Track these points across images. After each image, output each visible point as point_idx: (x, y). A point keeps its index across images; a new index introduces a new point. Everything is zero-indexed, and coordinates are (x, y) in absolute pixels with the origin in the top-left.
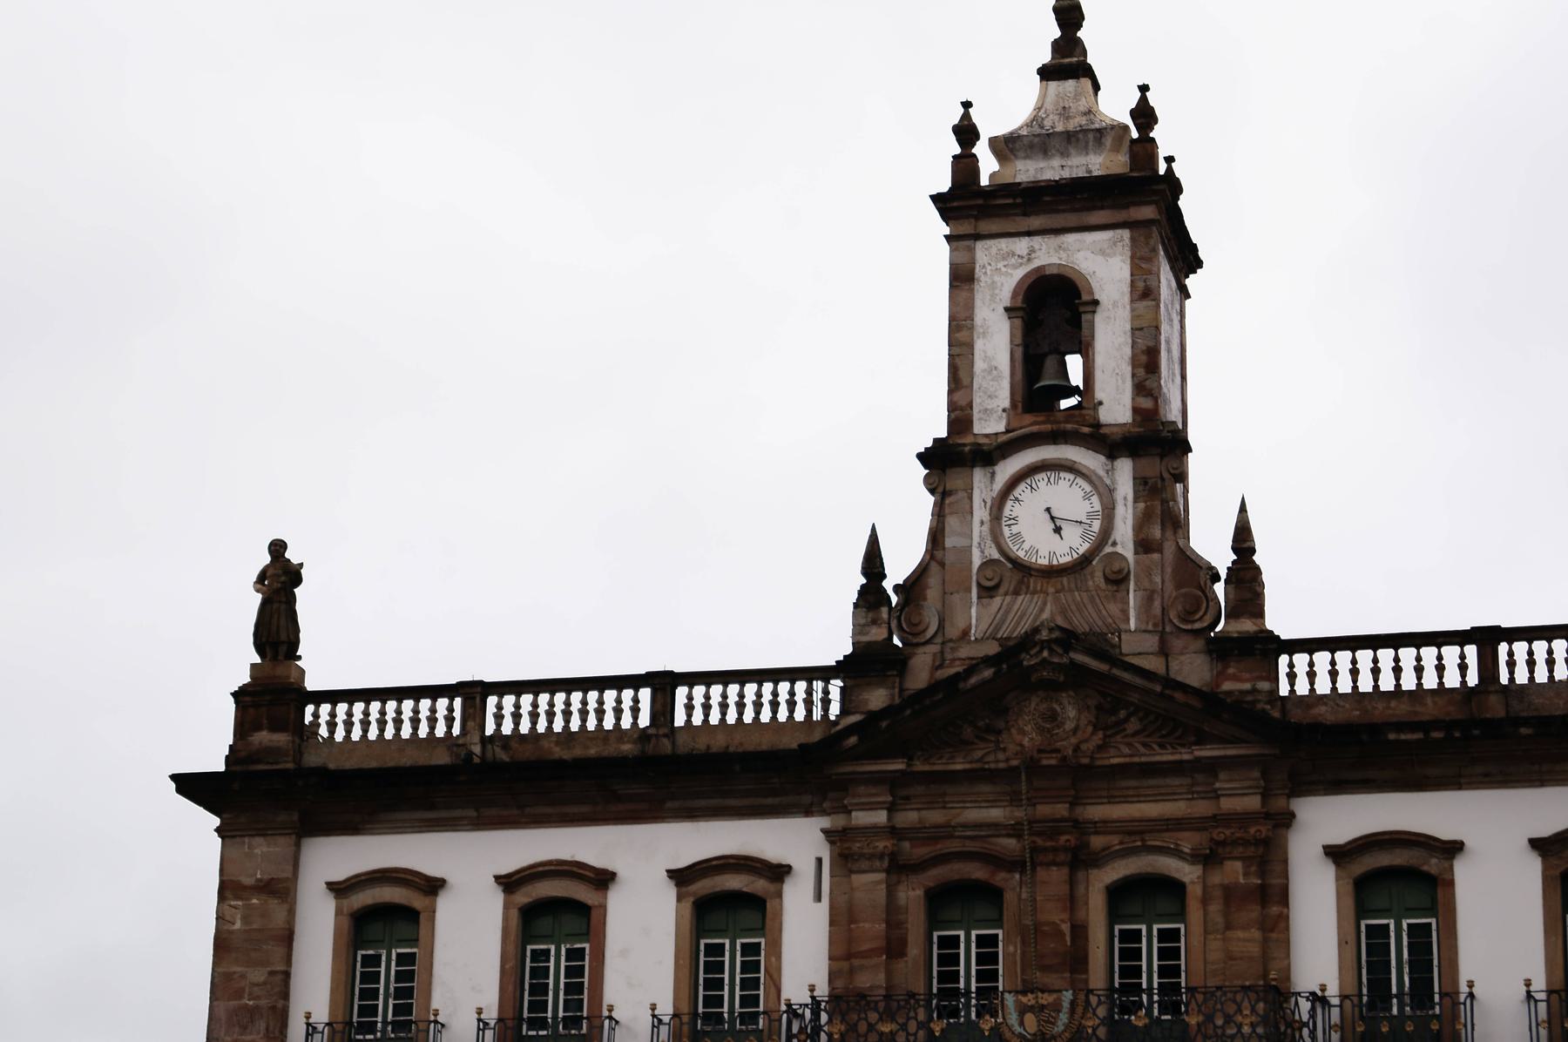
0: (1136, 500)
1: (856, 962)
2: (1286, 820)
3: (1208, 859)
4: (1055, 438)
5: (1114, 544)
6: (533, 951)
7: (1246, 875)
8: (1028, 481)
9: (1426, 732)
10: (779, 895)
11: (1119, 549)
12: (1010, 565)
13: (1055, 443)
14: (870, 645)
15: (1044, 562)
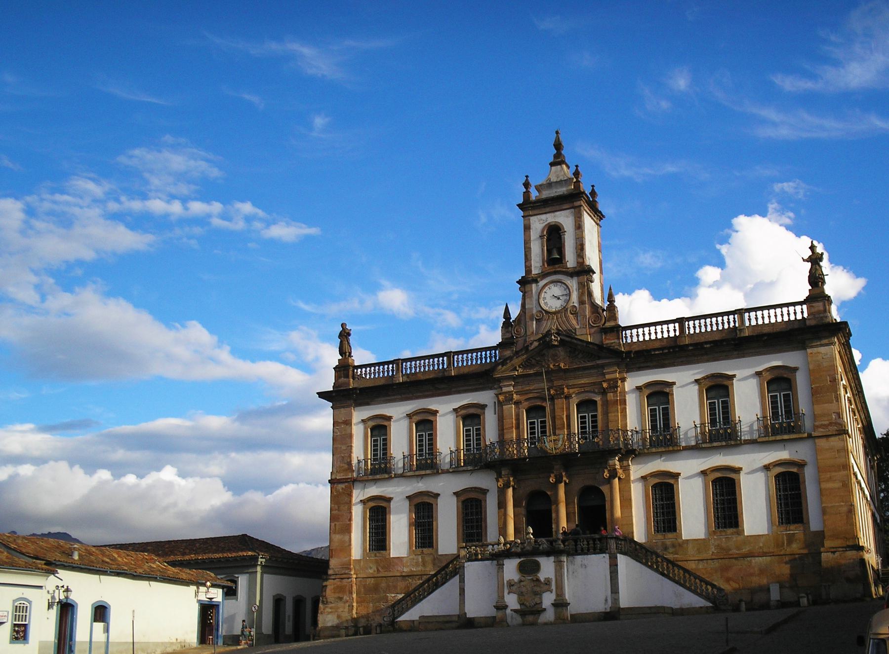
0: (579, 290)
2: (623, 380)
3: (604, 392)
4: (555, 273)
5: (573, 303)
7: (613, 397)
8: (548, 286)
9: (663, 350)
10: (484, 413)
12: (544, 312)
13: (555, 274)
14: (506, 339)
15: (554, 310)
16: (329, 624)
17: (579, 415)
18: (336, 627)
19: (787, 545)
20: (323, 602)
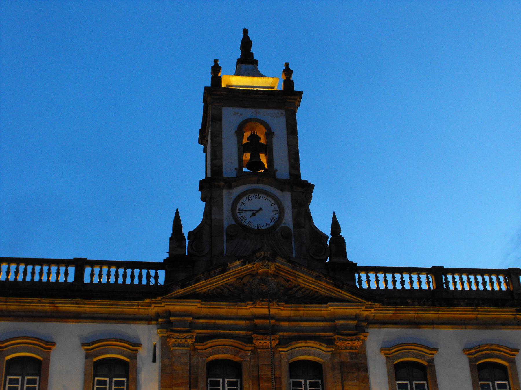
0: (293, 207)
6: (10, 379)
7: (351, 358)
11: (287, 225)
12: (241, 228)
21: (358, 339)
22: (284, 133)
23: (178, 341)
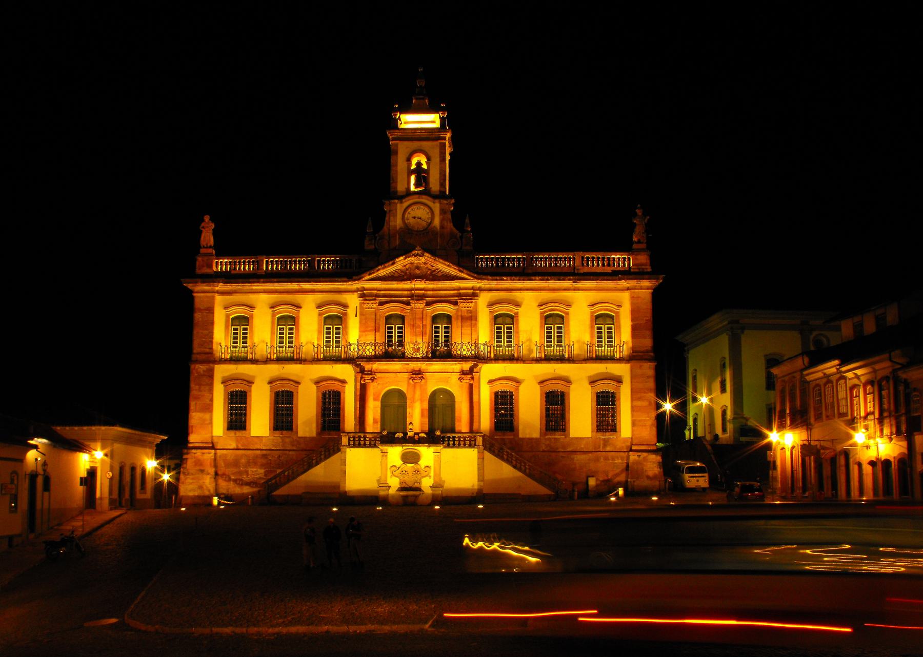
0: (441, 214)
1: (366, 333)
7: (467, 313)
15: (416, 229)
16: (191, 494)
17: (434, 325)
18: (199, 497)
19: (602, 448)
20: (184, 473)
21: (472, 302)
22: (438, 160)
23: (369, 305)
